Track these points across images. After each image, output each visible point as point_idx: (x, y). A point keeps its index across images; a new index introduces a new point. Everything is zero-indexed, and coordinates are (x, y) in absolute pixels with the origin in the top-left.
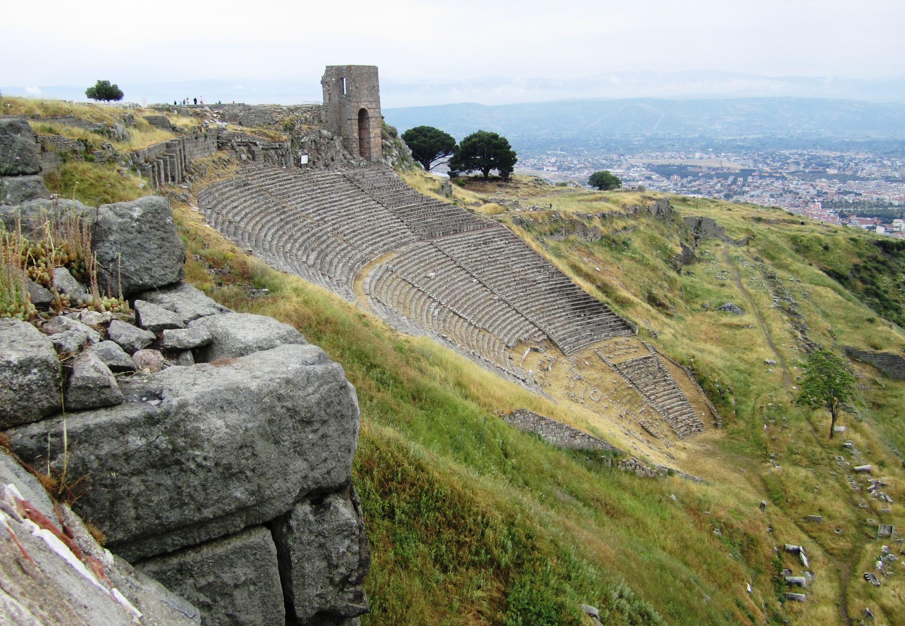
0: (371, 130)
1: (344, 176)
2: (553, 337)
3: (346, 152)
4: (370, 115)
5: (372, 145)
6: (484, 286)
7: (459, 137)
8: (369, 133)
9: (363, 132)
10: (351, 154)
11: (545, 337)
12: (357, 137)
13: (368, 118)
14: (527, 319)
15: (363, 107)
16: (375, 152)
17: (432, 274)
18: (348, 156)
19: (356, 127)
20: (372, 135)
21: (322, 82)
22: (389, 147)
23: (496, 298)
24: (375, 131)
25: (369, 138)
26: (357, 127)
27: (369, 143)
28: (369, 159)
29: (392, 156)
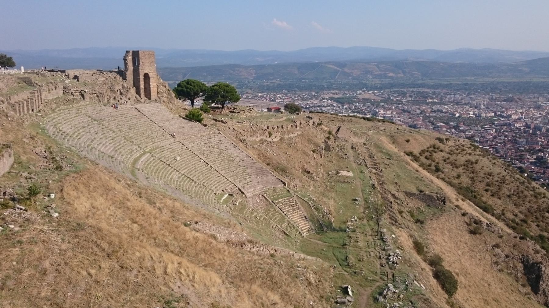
0: (151, 84)
2: (240, 188)
3: (137, 96)
4: (150, 76)
5: (151, 91)
6: (207, 163)
7: (209, 84)
9: (147, 85)
10: (140, 97)
11: (237, 189)
12: (143, 88)
13: (149, 78)
14: (228, 180)
15: (146, 72)
16: (154, 95)
20: (151, 86)
22: (162, 92)
24: (153, 85)
27: (150, 90)
28: (150, 99)
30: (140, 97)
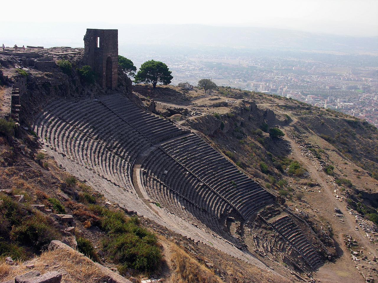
0: (113, 70)
1: (100, 102)
4: (112, 61)
8: (112, 72)
10: (101, 86)
13: (111, 63)
15: (109, 56)
17: (166, 172)
18: (100, 88)
19: (104, 69)
20: (113, 73)
21: (84, 39)
23: (202, 184)
24: (115, 71)
25: (112, 75)
26: (105, 69)
29: (123, 85)
30: (101, 86)
